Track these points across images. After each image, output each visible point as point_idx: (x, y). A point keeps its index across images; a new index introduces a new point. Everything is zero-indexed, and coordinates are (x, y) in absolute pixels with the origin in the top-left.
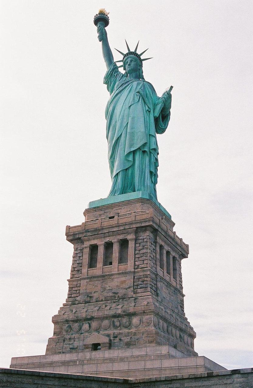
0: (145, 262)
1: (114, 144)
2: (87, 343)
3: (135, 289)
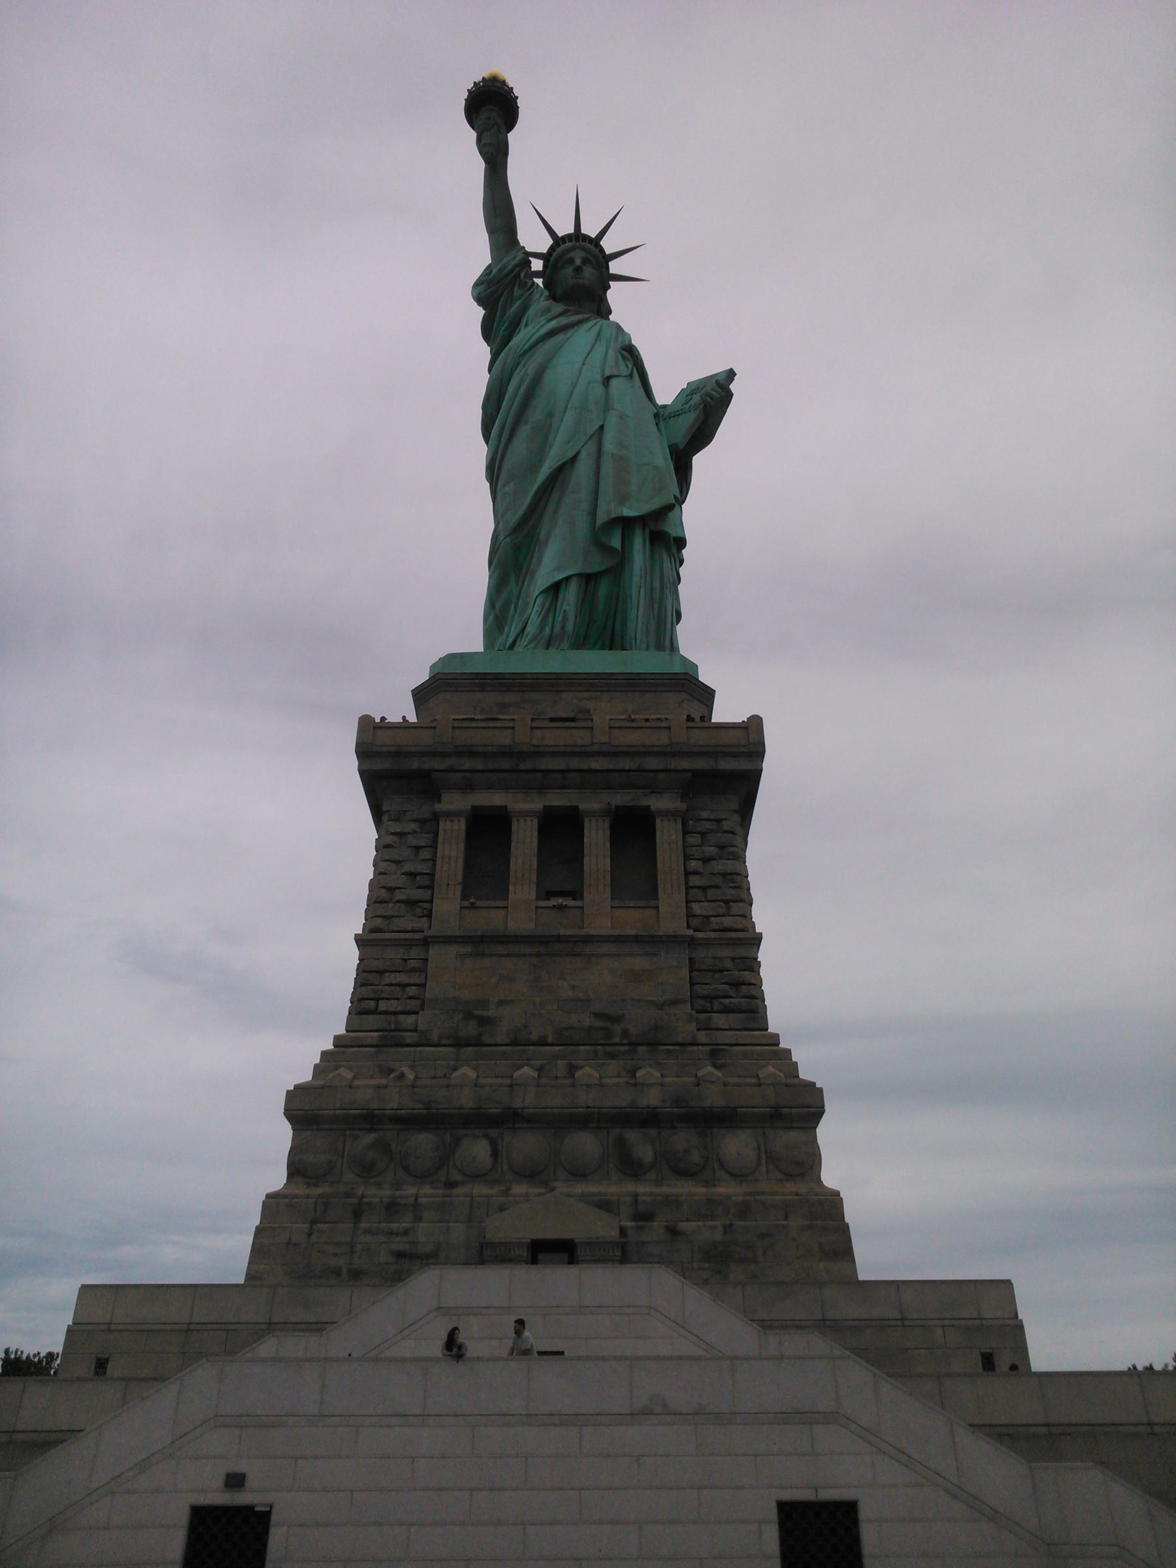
0: (735, 909)
1: (539, 488)
3: (698, 1012)
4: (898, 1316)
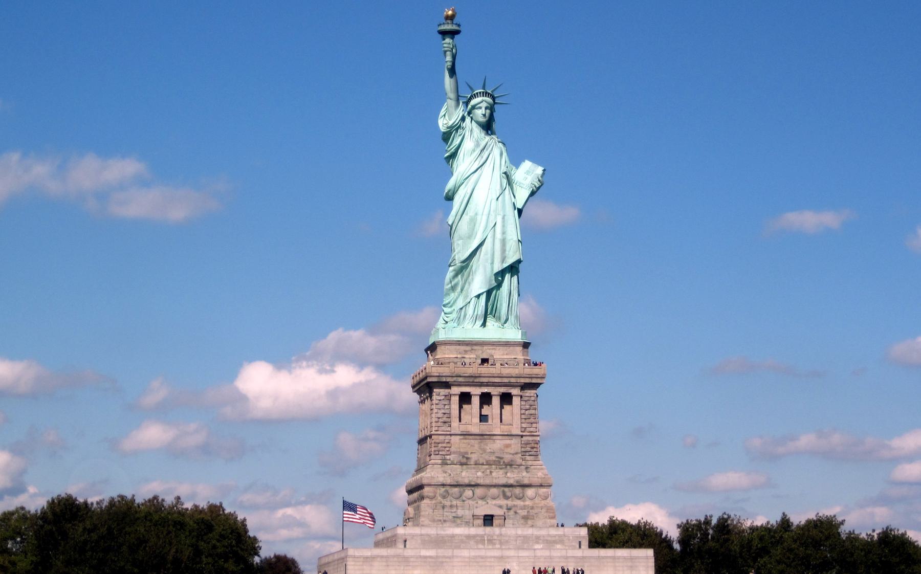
0: (534, 425)
2: (477, 514)
4: (562, 533)
